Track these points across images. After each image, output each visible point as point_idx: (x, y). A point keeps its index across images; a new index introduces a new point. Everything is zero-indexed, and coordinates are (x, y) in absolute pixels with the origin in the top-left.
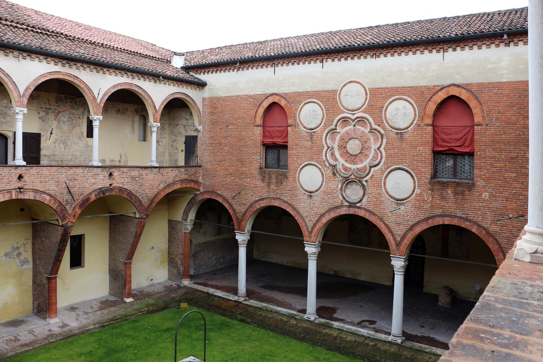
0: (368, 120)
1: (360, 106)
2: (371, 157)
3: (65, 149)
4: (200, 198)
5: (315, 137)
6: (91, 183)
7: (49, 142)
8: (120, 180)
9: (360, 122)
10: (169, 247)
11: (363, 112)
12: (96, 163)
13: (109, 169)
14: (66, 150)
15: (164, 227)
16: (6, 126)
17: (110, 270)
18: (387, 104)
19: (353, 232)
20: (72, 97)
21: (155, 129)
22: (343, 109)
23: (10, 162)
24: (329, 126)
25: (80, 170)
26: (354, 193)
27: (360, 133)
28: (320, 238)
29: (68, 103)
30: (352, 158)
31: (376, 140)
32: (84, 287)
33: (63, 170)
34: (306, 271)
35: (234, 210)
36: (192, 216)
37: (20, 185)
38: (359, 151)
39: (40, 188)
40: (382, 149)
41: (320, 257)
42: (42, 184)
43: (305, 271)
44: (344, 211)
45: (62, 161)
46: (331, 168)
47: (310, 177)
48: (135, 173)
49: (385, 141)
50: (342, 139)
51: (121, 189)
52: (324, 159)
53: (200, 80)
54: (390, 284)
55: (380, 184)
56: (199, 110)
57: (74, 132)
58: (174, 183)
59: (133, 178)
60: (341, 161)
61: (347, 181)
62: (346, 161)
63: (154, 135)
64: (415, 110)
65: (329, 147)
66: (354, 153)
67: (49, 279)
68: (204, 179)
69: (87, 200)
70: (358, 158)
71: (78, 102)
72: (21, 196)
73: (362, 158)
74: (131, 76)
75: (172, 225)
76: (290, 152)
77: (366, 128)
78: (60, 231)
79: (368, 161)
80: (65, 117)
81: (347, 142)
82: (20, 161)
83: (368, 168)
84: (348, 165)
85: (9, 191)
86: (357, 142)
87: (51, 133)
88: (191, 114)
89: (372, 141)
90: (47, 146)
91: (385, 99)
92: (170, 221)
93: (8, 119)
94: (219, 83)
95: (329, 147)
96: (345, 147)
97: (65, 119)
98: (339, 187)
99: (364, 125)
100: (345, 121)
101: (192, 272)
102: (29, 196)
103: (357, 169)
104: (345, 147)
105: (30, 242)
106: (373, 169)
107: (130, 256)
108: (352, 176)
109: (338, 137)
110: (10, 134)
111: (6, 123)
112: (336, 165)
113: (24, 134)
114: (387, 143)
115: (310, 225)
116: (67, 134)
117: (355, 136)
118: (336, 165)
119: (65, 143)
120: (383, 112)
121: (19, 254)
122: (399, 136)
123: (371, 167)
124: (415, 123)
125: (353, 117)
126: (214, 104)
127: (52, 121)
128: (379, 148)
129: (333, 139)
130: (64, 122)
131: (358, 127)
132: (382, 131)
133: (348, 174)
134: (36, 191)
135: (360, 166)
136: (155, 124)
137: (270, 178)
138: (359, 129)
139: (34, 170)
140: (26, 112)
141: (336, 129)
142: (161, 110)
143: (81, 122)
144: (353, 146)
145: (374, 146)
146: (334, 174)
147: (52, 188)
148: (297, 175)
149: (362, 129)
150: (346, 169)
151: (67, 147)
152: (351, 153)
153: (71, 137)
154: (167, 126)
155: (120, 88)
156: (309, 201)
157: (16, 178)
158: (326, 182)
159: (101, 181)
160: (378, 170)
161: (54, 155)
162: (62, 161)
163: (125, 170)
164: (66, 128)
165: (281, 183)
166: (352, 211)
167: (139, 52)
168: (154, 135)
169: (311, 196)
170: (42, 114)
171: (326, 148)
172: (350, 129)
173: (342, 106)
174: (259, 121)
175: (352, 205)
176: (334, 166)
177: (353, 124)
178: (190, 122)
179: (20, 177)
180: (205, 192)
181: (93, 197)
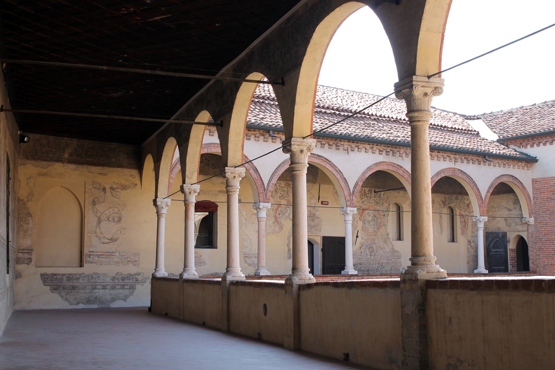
3: (371, 255)
14: (372, 257)
16: (315, 230)
20: (377, 190)
29: (373, 198)
45: (368, 271)
53: (526, 155)
56: (529, 196)
57: (379, 234)
71: (382, 195)
74: (448, 158)
80: (369, 216)
87: (357, 237)
93: (316, 221)
97: (370, 219)
111: (314, 226)
116: (372, 237)
127: (357, 222)
130: (369, 222)
136: (482, 217)
140: (356, 212)
142: (487, 200)
143: (386, 221)
151: (373, 253)
153: (376, 241)
155: (443, 176)
161: (360, 264)
162: (368, 271)
167: (443, 126)
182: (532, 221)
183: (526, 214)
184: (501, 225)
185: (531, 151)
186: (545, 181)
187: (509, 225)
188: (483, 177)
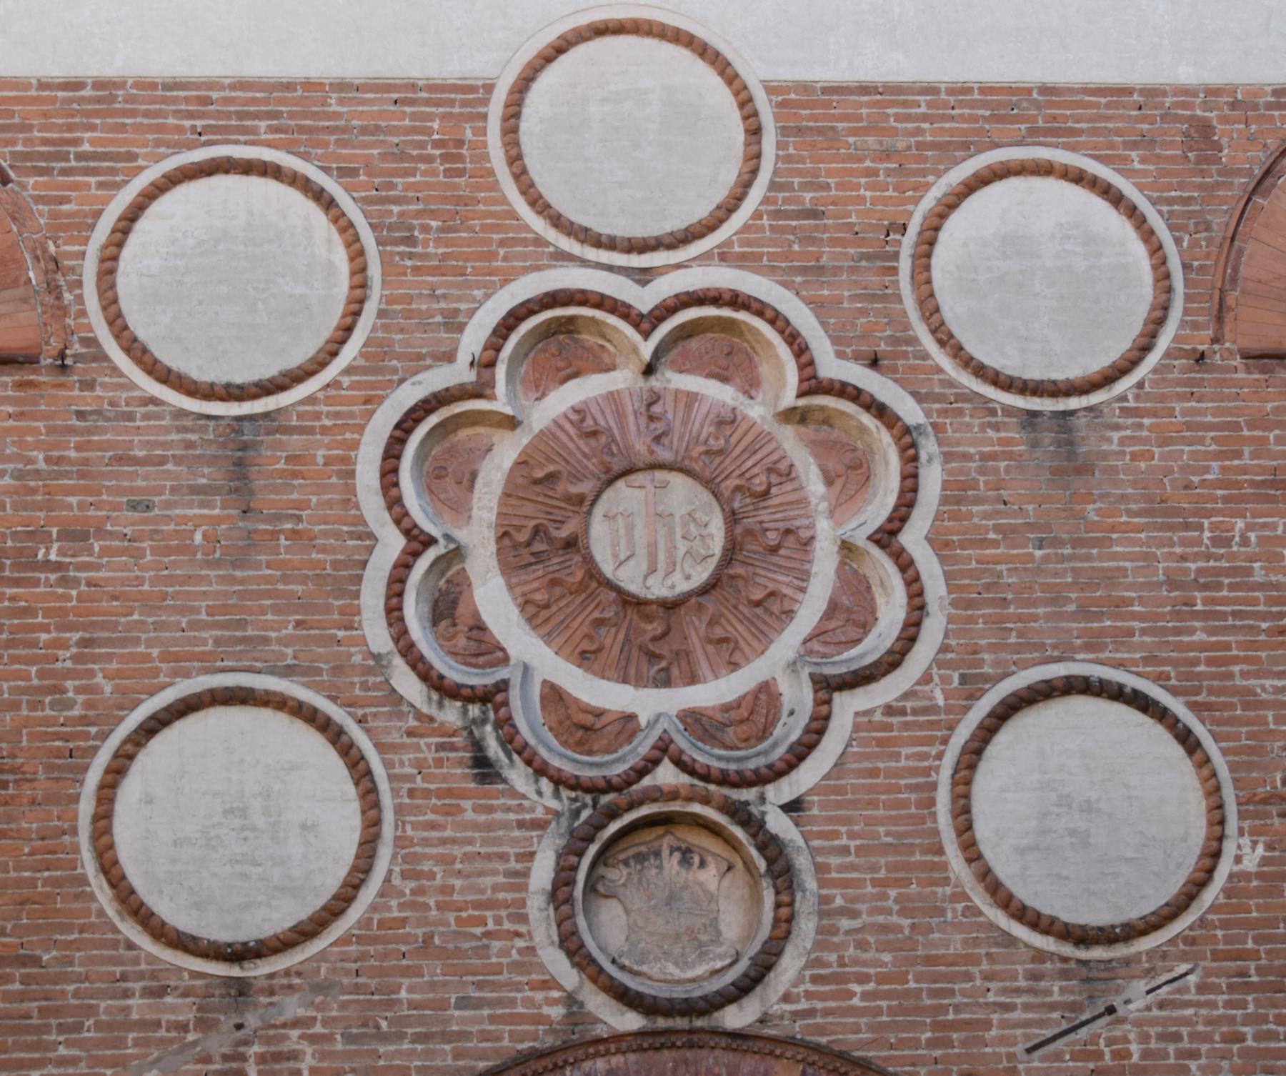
0: (776, 319)
1: (701, 211)
2: (809, 613)
5: (272, 458)
9: (694, 344)
11: (723, 256)
18: (929, 201)
22: (551, 235)
24: (417, 362)
27: (699, 421)
30: (649, 634)
31: (850, 473)
38: (701, 575)
40: (913, 538)
46: (451, 714)
49: (932, 480)
50: (533, 479)
52: (378, 636)
55: (928, 816)
60: (535, 657)
61: (613, 814)
62: (585, 658)
64: (1156, 250)
65: (418, 541)
66: (658, 589)
70: (694, 629)
73: (740, 631)
77: (750, 386)
81: (583, 504)
83: (798, 697)
86: (681, 493)
89: (815, 486)
91: (910, 169)
95: (418, 541)
96: (571, 544)
98: (543, 872)
99: (736, 364)
100: (557, 334)
103: (694, 720)
104: (571, 544)
106: (847, 706)
108: (666, 775)
112: (503, 686)
114: (955, 493)
117: (664, 455)
118: (503, 686)
120: (905, 265)
122: (1048, 437)
123: (828, 687)
124: (1164, 342)
125: (645, 299)
128: (886, 537)
129: (451, 479)
131: (675, 380)
132: (910, 411)
138: (692, 398)
141: (480, 391)
144: (652, 538)
145: (831, 528)
146: (484, 769)
148: (86, 807)
149: (721, 394)
150: (583, 727)
152: (634, 587)
156: (219, 1043)
158: (400, 842)
160: (889, 710)
169: (242, 989)
171: (392, 544)
172: (613, 397)
173: (538, 203)
176: (491, 697)
177: (647, 349)
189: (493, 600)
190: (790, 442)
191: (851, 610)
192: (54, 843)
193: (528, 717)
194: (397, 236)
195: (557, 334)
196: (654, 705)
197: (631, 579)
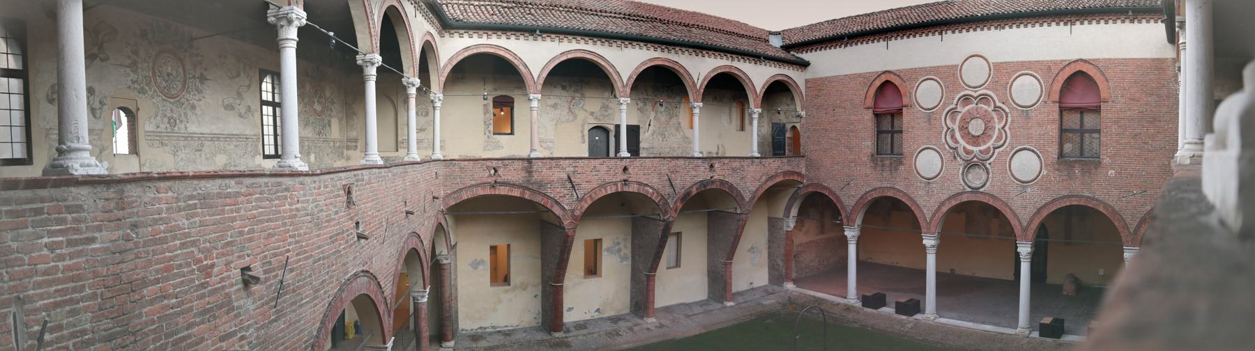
4: (803, 192)
6: (689, 178)
7: (647, 134)
8: (721, 172)
10: (769, 248)
12: (697, 155)
13: (710, 160)
15: (764, 225)
17: (709, 272)
19: (976, 219)
21: (756, 116)
23: (612, 154)
25: (681, 162)
26: (976, 178)
28: (939, 230)
30: (975, 140)
31: (1000, 118)
32: (682, 283)
33: (665, 162)
34: (925, 272)
35: (841, 202)
36: (794, 212)
37: (625, 177)
39: (643, 180)
41: (940, 251)
42: (646, 177)
43: (923, 273)
44: (965, 198)
47: (928, 162)
48: (736, 164)
50: (963, 119)
51: (722, 182)
54: (1011, 277)
58: (776, 175)
59: (734, 170)
63: (755, 123)
67: (648, 276)
68: (807, 170)
69: (689, 193)
72: (626, 189)
75: (773, 224)
76: (904, 135)
78: (661, 226)
79: (992, 141)
82: (624, 153)
84: (970, 147)
85: (615, 183)
86: (980, 121)
88: (793, 99)
90: (645, 138)
92: (770, 218)
94: (825, 63)
99: (988, 103)
100: (966, 99)
101: (794, 275)
102: (633, 188)
105: (629, 238)
107: (731, 255)
109: (959, 117)
110: (612, 128)
113: (628, 127)
114: (1012, 121)
115: (928, 217)
119: (663, 135)
121: (619, 250)
126: (815, 85)
129: (953, 120)
133: (970, 157)
134: (640, 184)
135: (983, 147)
137: (883, 165)
139: (638, 162)
144: (976, 127)
145: (998, 126)
147: (654, 181)
150: (967, 152)
154: (765, 114)
157: (621, 170)
159: (703, 174)
163: (726, 161)
164: (663, 118)
165: (896, 170)
166: (973, 198)
168: (755, 123)
170: (641, 104)
174: (870, 102)
175: (975, 190)
176: (956, 149)
178: (792, 107)
179: (625, 169)
180: (808, 186)
181: (694, 191)
182: (803, 113)
183: (799, 109)
184: (782, 118)
185: (806, 56)
186: (815, 81)
187: (787, 117)
188: (758, 76)
189: (958, 135)
190: (994, 114)
191: (999, 138)
192: (910, 166)
193: (961, 151)
194: (947, 87)
195: (966, 99)
196: (976, 149)
197: (973, 133)
